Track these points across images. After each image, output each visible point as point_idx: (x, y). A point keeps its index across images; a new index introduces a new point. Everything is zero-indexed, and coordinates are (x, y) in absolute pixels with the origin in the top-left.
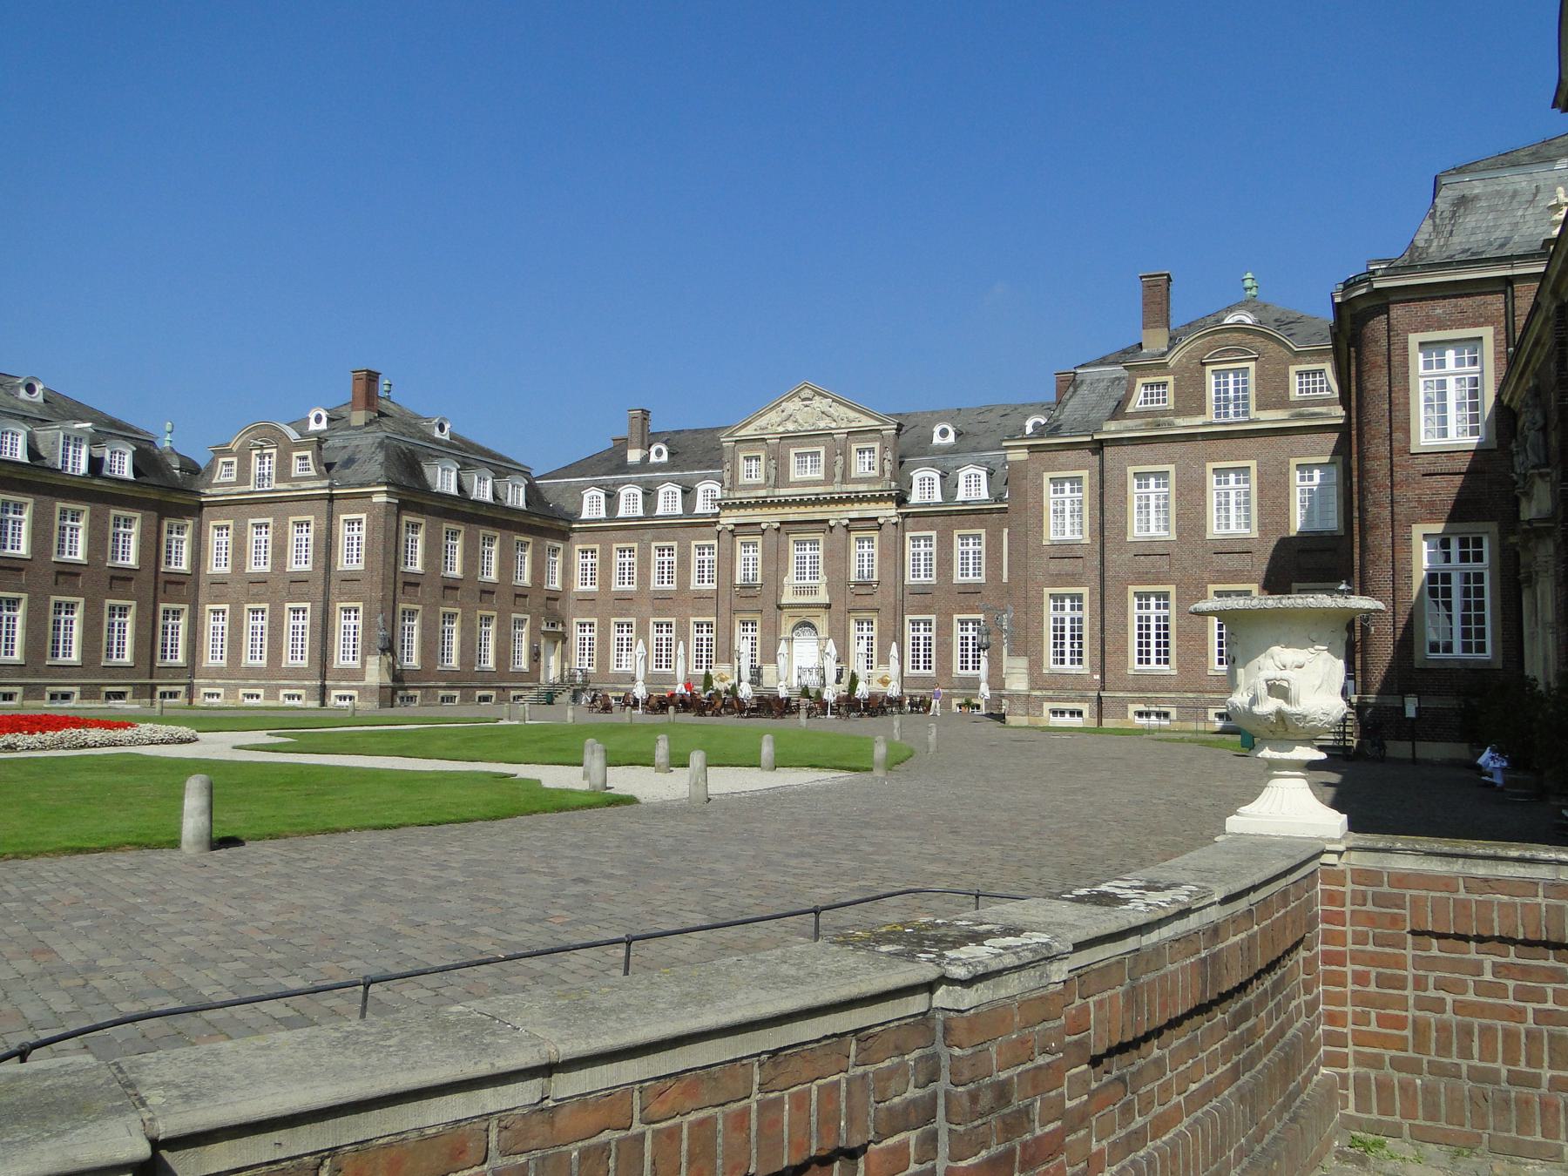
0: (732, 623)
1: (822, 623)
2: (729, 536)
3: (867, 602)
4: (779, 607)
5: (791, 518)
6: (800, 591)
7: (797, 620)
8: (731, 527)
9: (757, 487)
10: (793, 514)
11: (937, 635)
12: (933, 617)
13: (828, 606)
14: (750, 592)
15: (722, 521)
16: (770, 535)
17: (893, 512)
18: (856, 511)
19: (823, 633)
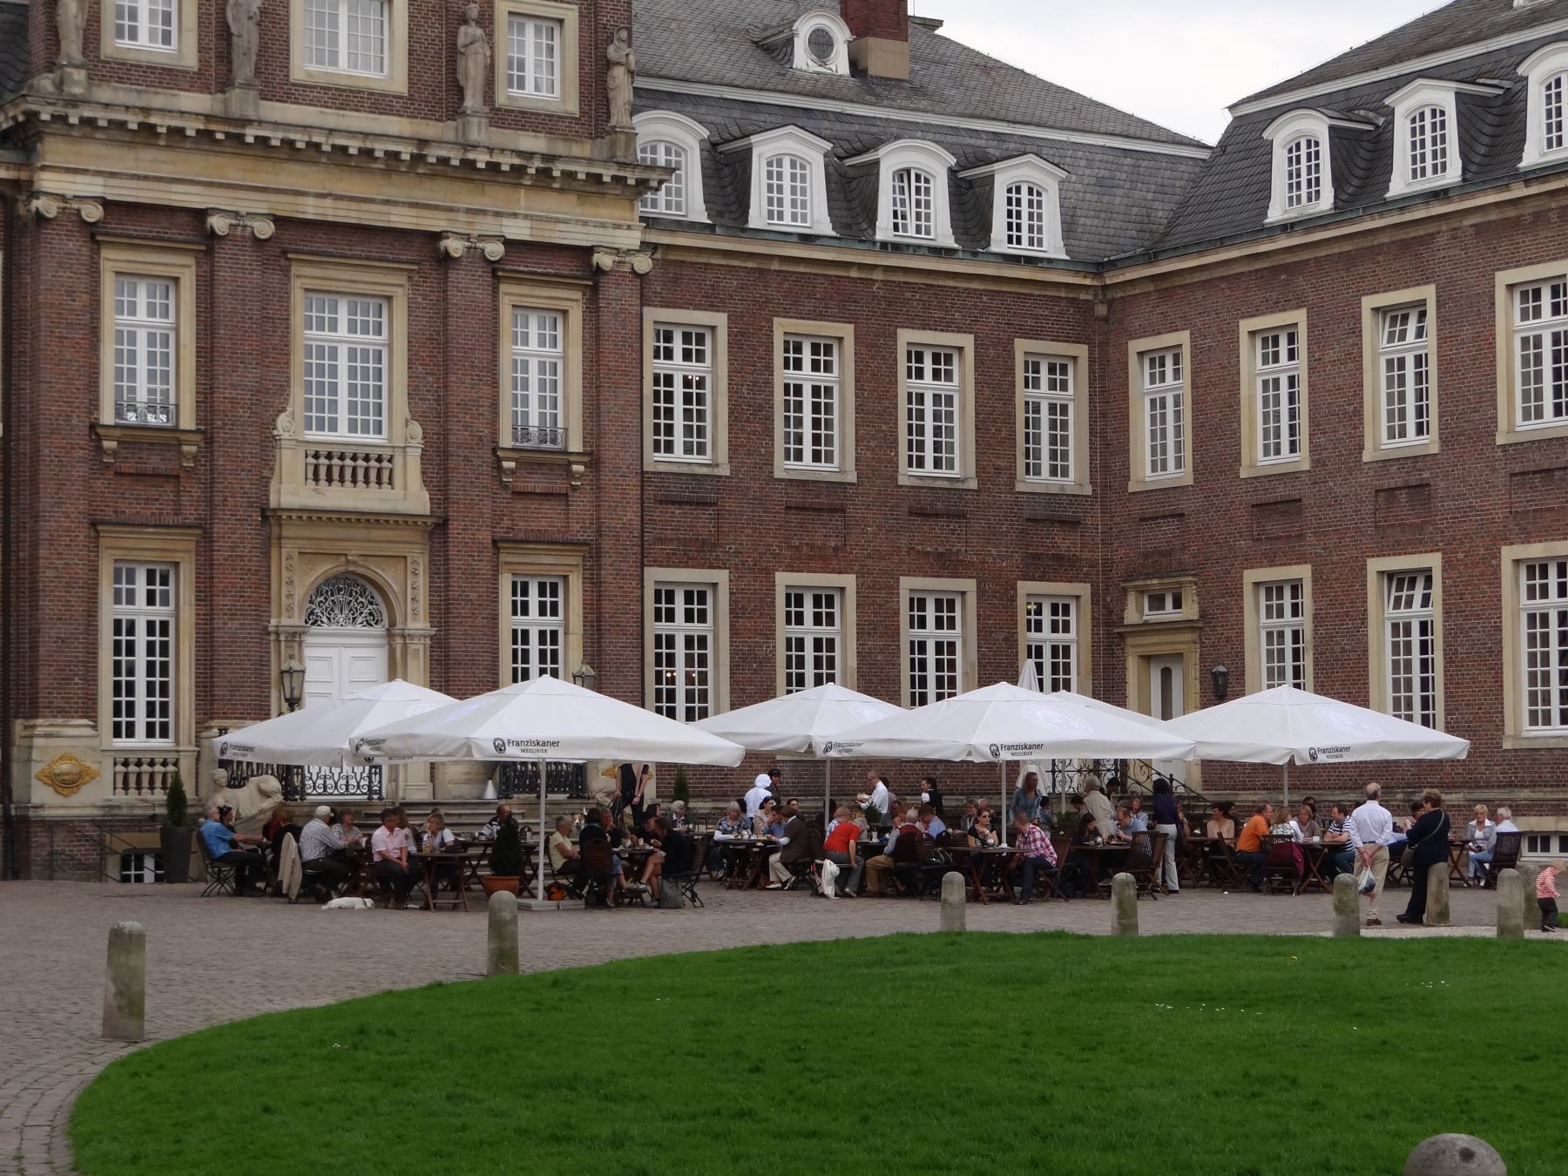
0: (94, 570)
1: (411, 588)
2: (75, 245)
3: (546, 518)
4: (269, 517)
5: (311, 209)
6: (329, 466)
7: (324, 568)
8: (93, 213)
9: (166, 76)
10: (319, 196)
11: (734, 632)
12: (722, 577)
13: (437, 529)
14: (155, 462)
15: (48, 182)
16: (236, 272)
17: (632, 239)
18: (525, 218)
19: (419, 623)
